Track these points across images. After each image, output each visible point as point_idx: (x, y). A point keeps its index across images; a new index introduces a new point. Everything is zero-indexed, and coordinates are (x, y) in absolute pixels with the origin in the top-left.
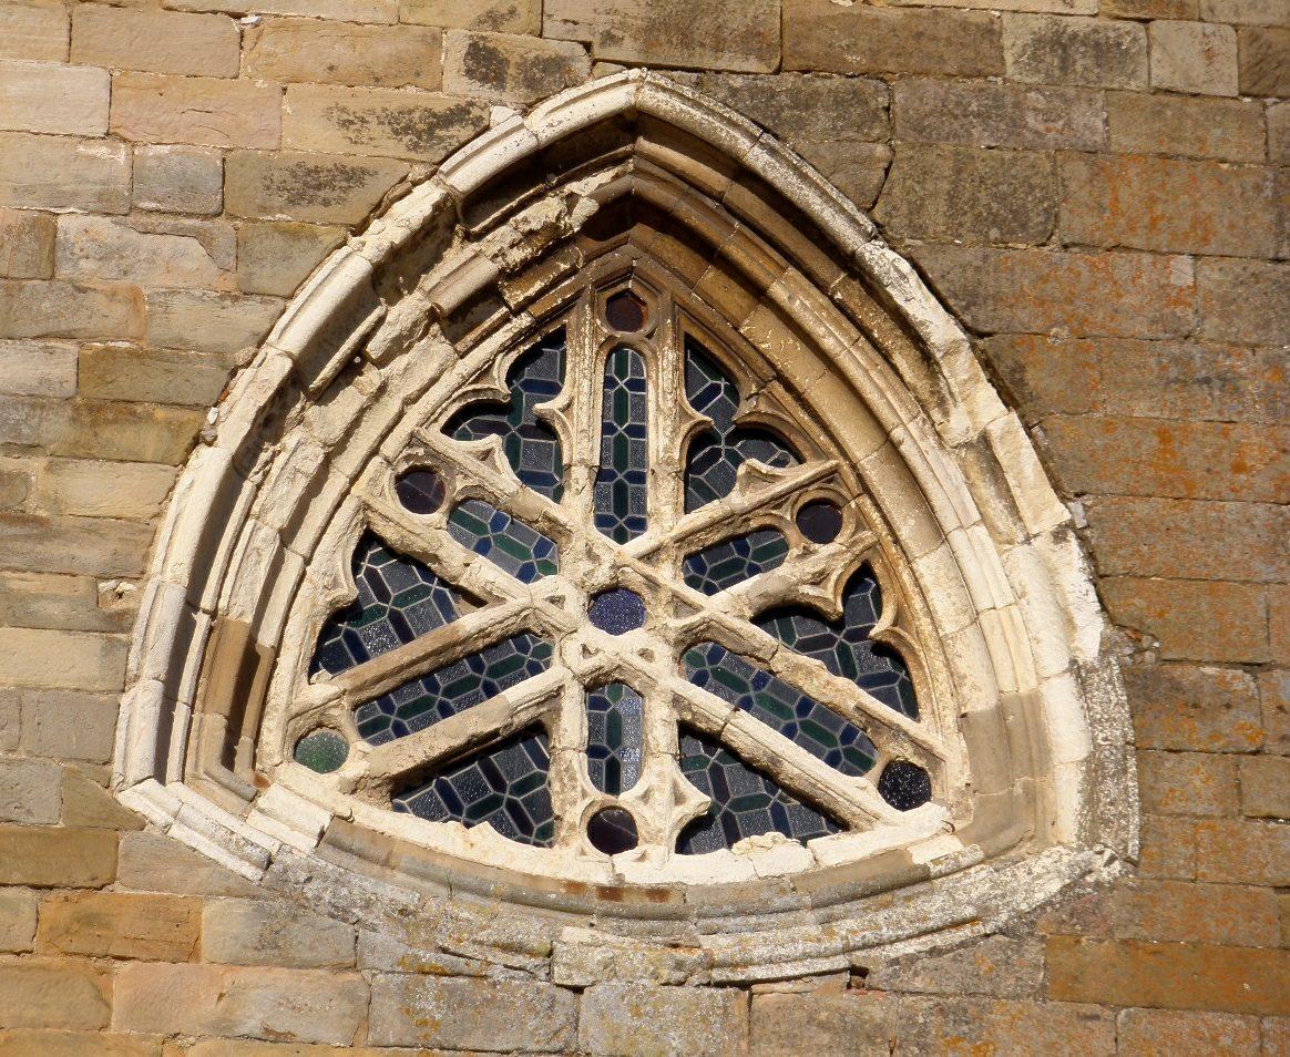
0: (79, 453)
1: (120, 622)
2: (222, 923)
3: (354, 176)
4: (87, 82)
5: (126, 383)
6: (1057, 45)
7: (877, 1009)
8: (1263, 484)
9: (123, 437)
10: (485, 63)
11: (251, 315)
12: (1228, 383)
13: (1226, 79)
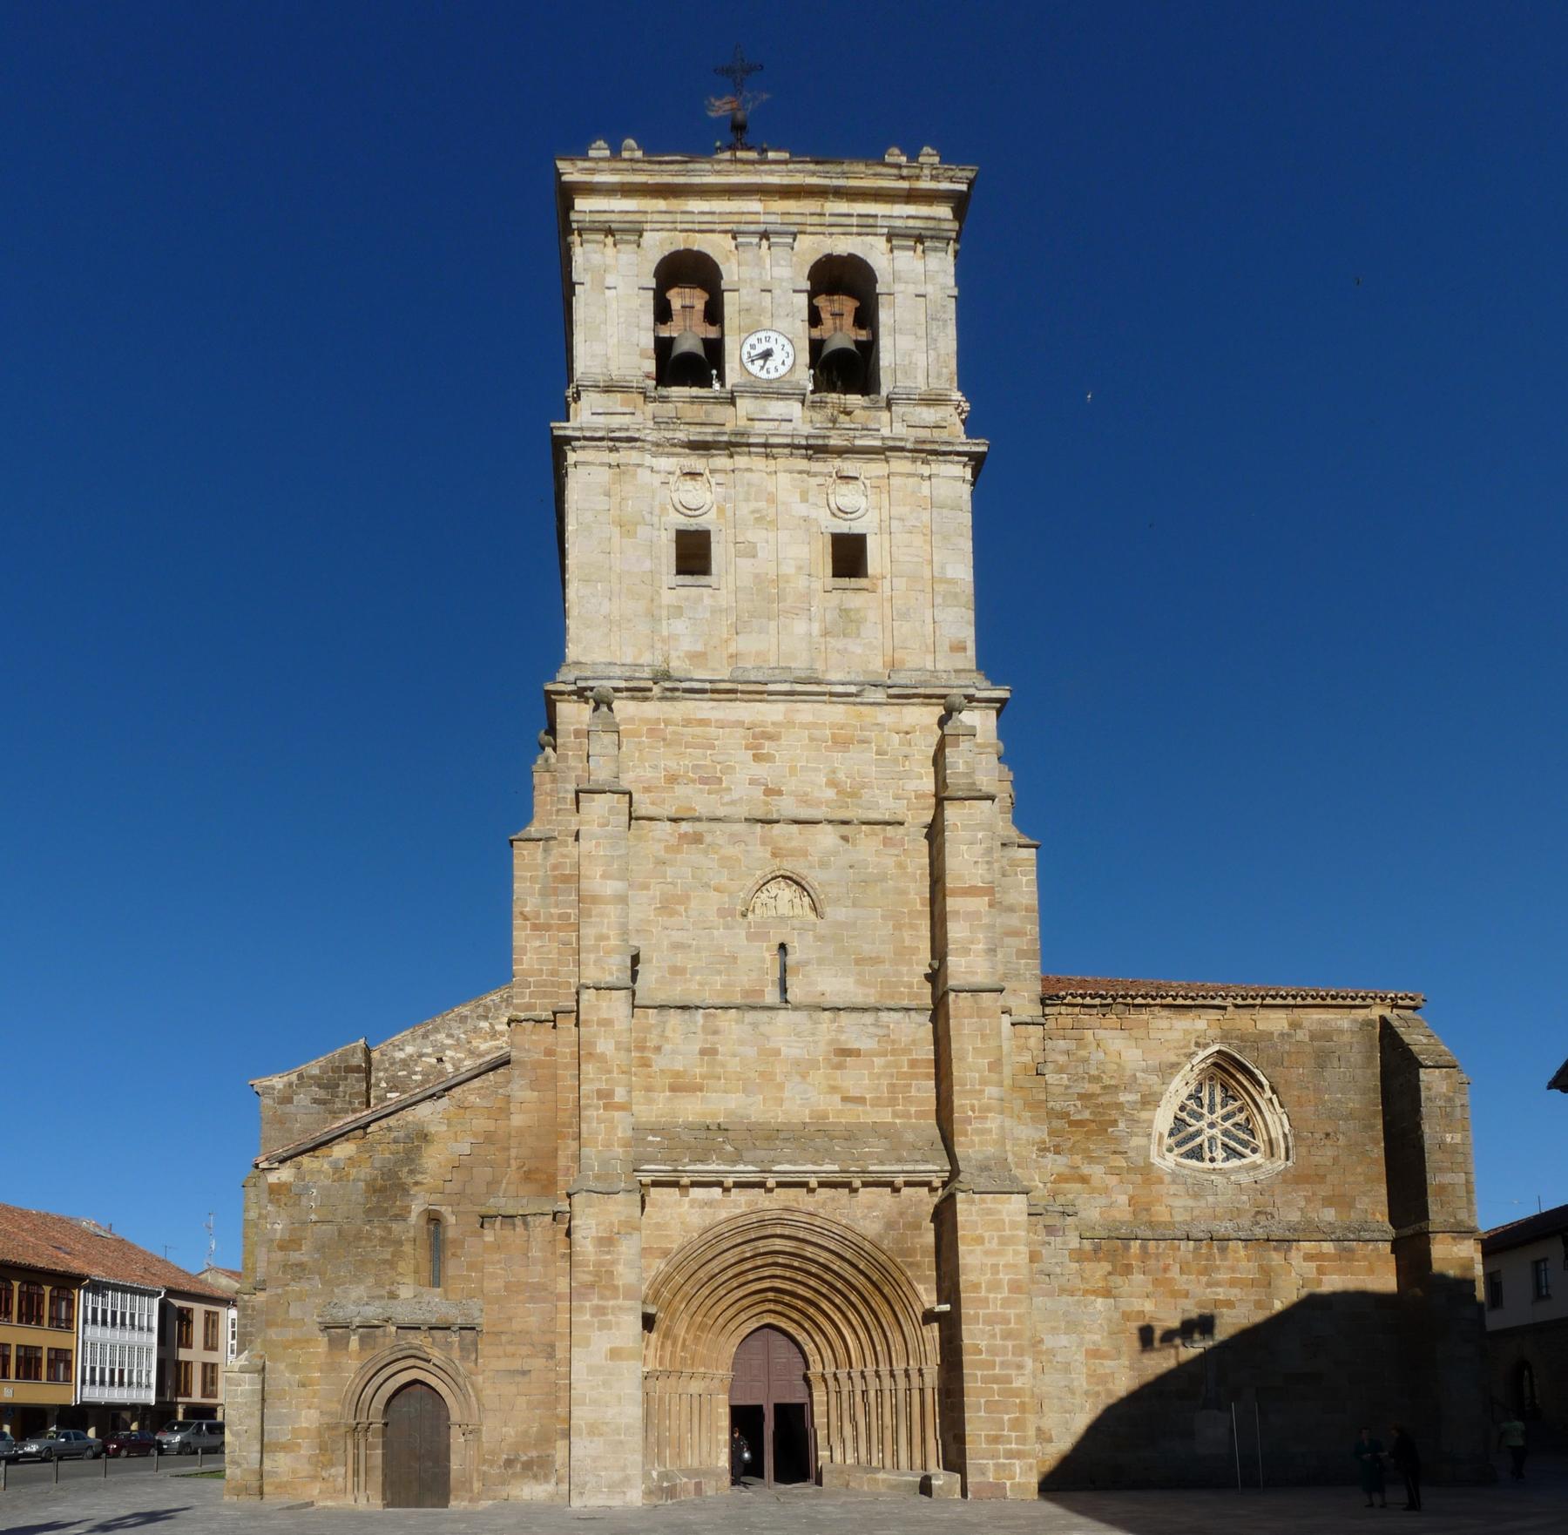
0: (1142, 1110)
1: (1150, 1135)
2: (1167, 1179)
3: (1179, 1064)
4: (1139, 1052)
5: (1149, 1099)
6: (1282, 1035)
7: (1258, 1186)
8: (1313, 1103)
9: (1148, 1107)
10: (1197, 1044)
11: (1164, 1087)
12: (1308, 1088)
13: (1307, 1039)
